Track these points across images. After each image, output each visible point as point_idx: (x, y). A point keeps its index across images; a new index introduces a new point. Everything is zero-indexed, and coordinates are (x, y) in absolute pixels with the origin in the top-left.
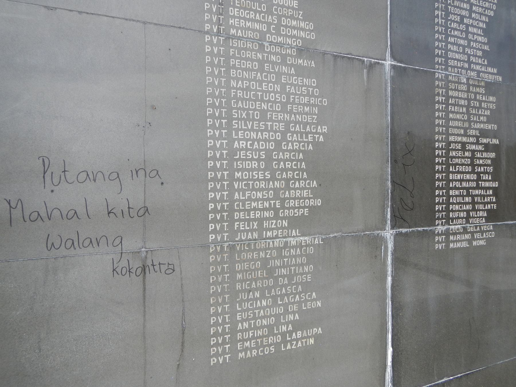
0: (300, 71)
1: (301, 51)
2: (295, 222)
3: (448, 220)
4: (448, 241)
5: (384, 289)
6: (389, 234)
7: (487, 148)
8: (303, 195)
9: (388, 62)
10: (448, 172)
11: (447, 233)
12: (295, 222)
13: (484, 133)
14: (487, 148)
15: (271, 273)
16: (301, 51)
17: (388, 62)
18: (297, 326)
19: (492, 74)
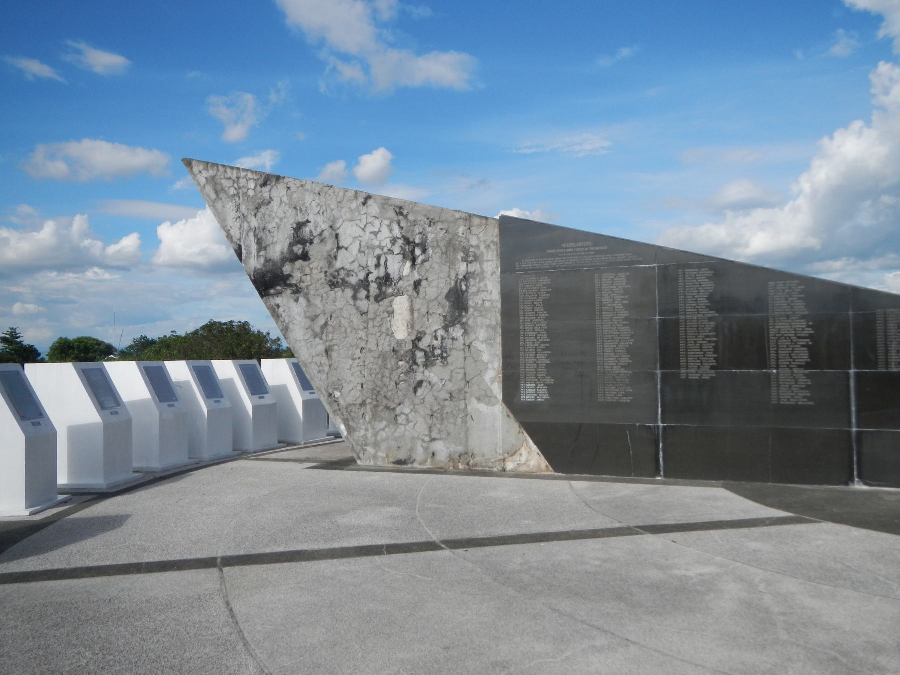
0: (624, 325)
1: (624, 320)
2: (623, 367)
3: (687, 368)
4: (687, 376)
5: (657, 389)
6: (659, 372)
7: (710, 342)
8: (626, 359)
9: (658, 318)
10: (687, 351)
11: (687, 374)
12: (623, 367)
13: (707, 337)
14: (710, 342)
15: (615, 380)
16: (624, 320)
17: (658, 318)
18: (624, 396)
19: (713, 314)
